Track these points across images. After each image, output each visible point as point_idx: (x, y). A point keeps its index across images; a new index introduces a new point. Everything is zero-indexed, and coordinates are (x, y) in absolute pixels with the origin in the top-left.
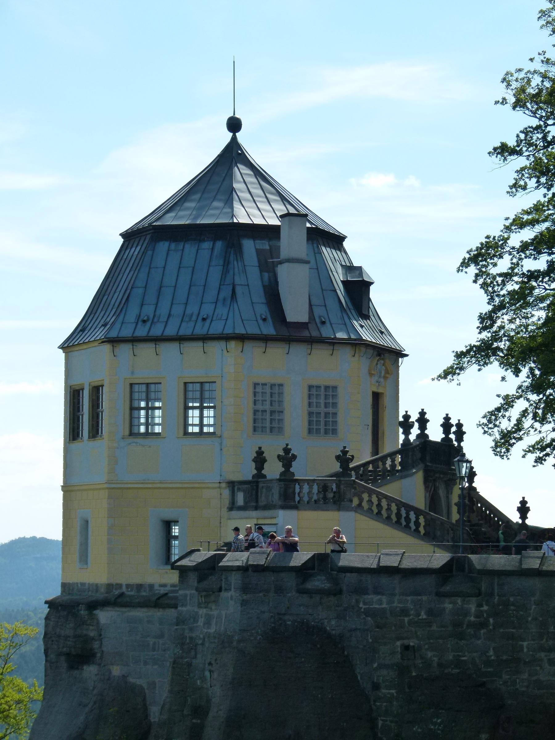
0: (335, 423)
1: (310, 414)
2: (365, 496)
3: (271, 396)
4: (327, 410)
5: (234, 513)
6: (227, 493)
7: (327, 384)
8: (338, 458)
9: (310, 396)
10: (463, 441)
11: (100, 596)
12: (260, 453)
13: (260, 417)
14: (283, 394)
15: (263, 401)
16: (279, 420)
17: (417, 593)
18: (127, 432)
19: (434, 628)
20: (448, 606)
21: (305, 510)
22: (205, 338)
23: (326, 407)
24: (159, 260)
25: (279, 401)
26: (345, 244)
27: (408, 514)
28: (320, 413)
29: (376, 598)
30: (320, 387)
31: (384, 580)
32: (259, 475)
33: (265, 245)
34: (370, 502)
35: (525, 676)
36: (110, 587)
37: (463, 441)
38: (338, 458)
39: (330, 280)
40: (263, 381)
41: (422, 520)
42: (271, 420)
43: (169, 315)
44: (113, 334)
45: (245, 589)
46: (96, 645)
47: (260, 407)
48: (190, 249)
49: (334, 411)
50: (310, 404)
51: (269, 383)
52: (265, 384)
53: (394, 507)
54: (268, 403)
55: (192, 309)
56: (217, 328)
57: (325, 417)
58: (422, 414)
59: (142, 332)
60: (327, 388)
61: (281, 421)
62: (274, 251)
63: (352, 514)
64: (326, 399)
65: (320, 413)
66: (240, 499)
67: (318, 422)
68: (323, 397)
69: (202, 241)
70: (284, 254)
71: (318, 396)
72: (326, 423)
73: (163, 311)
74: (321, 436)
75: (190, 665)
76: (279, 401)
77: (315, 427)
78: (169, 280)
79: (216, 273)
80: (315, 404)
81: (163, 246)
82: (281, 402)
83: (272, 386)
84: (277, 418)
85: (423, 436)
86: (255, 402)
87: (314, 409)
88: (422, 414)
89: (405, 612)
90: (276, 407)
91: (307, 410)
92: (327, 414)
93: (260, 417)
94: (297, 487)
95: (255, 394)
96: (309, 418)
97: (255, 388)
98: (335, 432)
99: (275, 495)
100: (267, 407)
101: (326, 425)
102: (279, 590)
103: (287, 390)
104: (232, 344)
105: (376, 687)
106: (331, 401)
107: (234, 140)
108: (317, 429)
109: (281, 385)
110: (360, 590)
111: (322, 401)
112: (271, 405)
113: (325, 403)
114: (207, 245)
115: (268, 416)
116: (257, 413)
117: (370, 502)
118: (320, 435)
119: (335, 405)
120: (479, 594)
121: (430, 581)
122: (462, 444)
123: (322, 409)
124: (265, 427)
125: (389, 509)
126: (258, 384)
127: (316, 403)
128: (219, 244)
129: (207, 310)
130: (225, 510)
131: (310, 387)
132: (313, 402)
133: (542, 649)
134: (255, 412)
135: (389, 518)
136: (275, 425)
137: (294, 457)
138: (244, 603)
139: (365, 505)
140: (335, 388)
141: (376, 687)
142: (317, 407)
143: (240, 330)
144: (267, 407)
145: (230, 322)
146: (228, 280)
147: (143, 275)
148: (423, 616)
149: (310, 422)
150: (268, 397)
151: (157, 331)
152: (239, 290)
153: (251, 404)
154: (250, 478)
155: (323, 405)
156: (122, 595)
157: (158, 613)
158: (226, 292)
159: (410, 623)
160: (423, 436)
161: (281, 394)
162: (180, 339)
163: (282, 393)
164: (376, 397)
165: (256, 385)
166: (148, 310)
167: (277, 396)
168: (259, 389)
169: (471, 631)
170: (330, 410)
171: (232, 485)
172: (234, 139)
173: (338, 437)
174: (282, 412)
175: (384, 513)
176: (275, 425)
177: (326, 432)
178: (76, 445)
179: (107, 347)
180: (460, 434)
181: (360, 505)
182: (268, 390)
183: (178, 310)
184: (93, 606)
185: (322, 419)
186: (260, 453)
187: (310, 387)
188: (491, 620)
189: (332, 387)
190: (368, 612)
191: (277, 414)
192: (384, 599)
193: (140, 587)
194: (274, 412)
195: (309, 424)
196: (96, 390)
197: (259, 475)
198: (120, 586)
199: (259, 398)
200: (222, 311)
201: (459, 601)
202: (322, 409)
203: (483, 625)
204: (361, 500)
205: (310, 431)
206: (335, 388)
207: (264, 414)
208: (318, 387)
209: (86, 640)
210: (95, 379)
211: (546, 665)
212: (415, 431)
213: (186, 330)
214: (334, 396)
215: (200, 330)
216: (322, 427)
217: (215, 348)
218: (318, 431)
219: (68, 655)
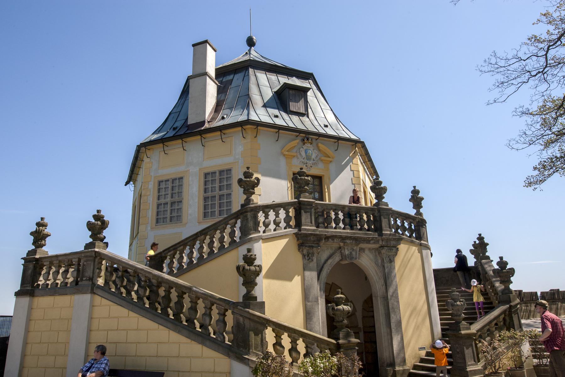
1: (206, 199)
3: (172, 190)
4: (221, 193)
10: (422, 207)
15: (165, 195)
16: (178, 209)
21: (42, 296)
23: (220, 190)
25: (178, 193)
28: (215, 196)
30: (215, 173)
37: (422, 207)
39: (248, 89)
50: (206, 191)
51: (171, 178)
52: (168, 180)
54: (169, 196)
60: (221, 172)
61: (180, 210)
64: (220, 182)
65: (215, 196)
67: (213, 206)
68: (217, 181)
71: (213, 181)
72: (220, 205)
77: (210, 210)
80: (210, 189)
82: (180, 193)
84: (177, 207)
87: (210, 194)
92: (221, 197)
93: (162, 209)
95: (159, 190)
96: (205, 203)
101: (220, 207)
106: (225, 183)
109: (181, 178)
111: (217, 185)
115: (169, 208)
116: (160, 207)
118: (216, 217)
122: (421, 210)
124: (166, 218)
126: (162, 181)
127: (212, 187)
131: (206, 175)
132: (208, 188)
136: (174, 214)
142: (212, 191)
144: (169, 199)
149: (205, 207)
150: (170, 192)
153: (156, 200)
155: (217, 189)
161: (181, 186)
163: (182, 185)
165: (160, 182)
167: (177, 188)
168: (163, 186)
170: (225, 192)
174: (181, 202)
182: (170, 185)
185: (217, 202)
187: (206, 175)
191: (176, 204)
195: (205, 209)
207: (166, 206)
208: (214, 173)
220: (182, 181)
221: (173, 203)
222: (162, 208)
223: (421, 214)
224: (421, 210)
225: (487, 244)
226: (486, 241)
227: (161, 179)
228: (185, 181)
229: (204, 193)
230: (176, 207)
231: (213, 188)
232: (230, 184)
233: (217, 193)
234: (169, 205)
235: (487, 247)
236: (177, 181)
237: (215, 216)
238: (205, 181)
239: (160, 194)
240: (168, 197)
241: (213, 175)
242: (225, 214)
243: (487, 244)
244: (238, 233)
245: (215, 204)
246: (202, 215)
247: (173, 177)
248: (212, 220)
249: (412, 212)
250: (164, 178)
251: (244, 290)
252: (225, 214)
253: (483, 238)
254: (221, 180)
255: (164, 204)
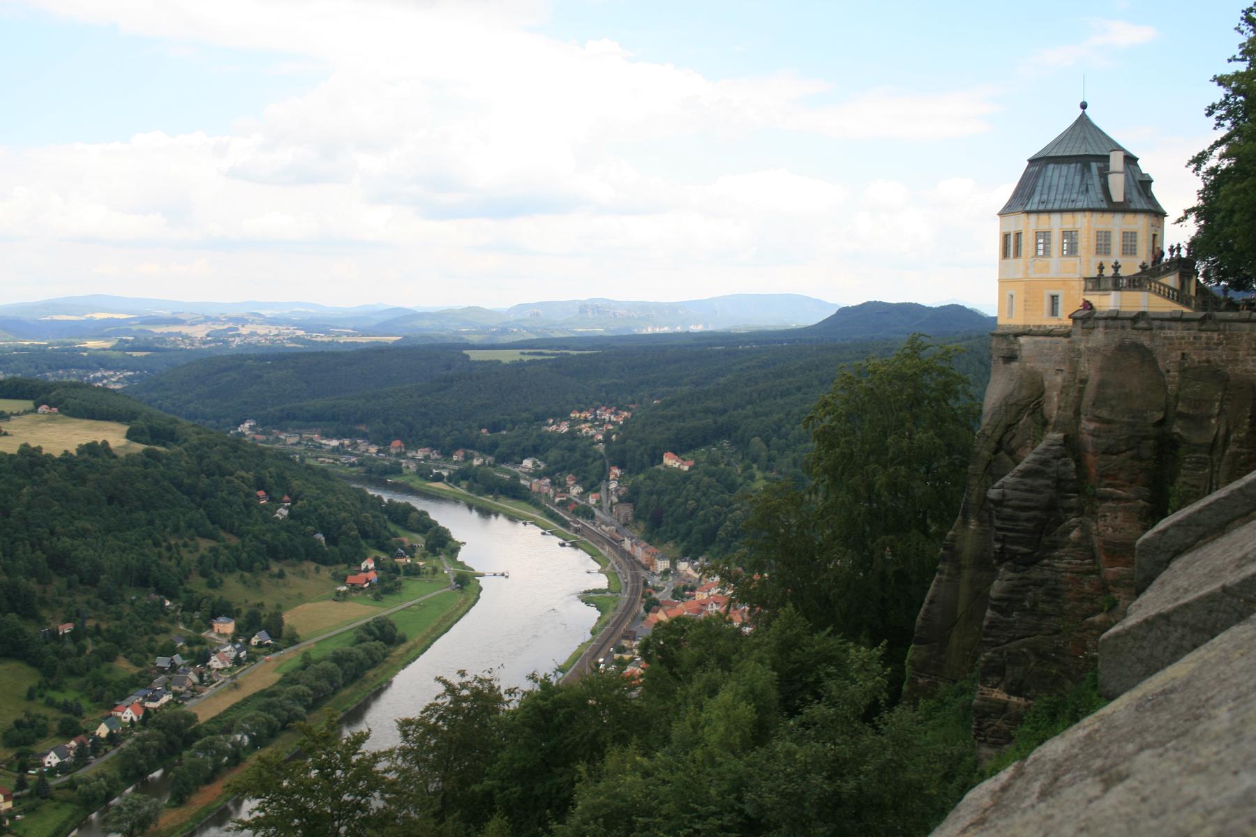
0: (1135, 249)
1: (1124, 245)
2: (1153, 284)
5: (1087, 292)
6: (1083, 283)
8: (1140, 266)
11: (1020, 330)
12: (1101, 264)
17: (1189, 329)
18: (1034, 254)
19: (1197, 345)
20: (1204, 335)
22: (1074, 211)
24: (1049, 173)
26: (1138, 162)
29: (1169, 331)
31: (1173, 324)
32: (1101, 275)
33: (1101, 165)
34: (1155, 287)
35: (1240, 367)
36: (1025, 326)
38: (1140, 266)
41: (1175, 294)
43: (1055, 200)
44: (1028, 208)
45: (1106, 327)
46: (1018, 353)
48: (1064, 168)
50: (1123, 241)
53: (1167, 290)
55: (1066, 196)
56: (1079, 205)
58: (1179, 245)
59: (1042, 207)
60: (1132, 233)
62: (1107, 168)
63: (1146, 293)
66: (1090, 286)
69: (1071, 163)
70: (1112, 169)
71: (1127, 237)
73: (1052, 197)
75: (1078, 361)
78: (1055, 182)
79: (1078, 179)
81: (1051, 166)
82: (1109, 240)
83: (1106, 232)
85: (1179, 255)
88: (1179, 245)
89: (1183, 338)
92: (1131, 245)
94: (1121, 281)
98: (1135, 254)
99: (1110, 283)
102: (1123, 327)
103: (1112, 235)
104: (1087, 214)
105: (1168, 371)
107: (1084, 112)
110: (1162, 328)
111: (1129, 239)
114: (1073, 165)
115: (1103, 247)
117: (1155, 287)
119: (1135, 241)
120: (1218, 330)
121: (1195, 324)
123: (1129, 243)
125: (1164, 291)
128: (1079, 165)
129: (1074, 196)
130: (1082, 292)
131: (1124, 233)
133: (1248, 355)
134: (1097, 245)
135: (1164, 295)
137: (1120, 266)
138: (1106, 333)
139: (1153, 288)
140: (1135, 233)
141: (1168, 371)
143: (1091, 206)
144: (1103, 242)
145: (1086, 202)
146: (1085, 182)
147: (1041, 181)
148: (1191, 340)
149: (1123, 249)
151: (1049, 207)
152: (1090, 187)
154: (1095, 276)
156: (1031, 330)
157: (1049, 339)
158: (1083, 188)
159: (1185, 343)
160: (1179, 255)
162: (1061, 211)
164: (1154, 236)
165: (1098, 232)
166: (1045, 197)
168: (1099, 234)
169: (1215, 347)
170: (1133, 243)
171: (1086, 279)
172: (1084, 112)
175: (1162, 292)
177: (1131, 254)
178: (1006, 261)
179: (1024, 216)
181: (1150, 289)
183: (1059, 197)
184: (1017, 335)
186: (1101, 264)
187: (1124, 233)
188: (1225, 342)
190: (1165, 338)
192: (1173, 332)
193: (1039, 326)
196: (1018, 235)
197: (1101, 275)
198: (1029, 326)
199: (1099, 238)
200: (1081, 197)
201: (1209, 333)
203: (1221, 344)
204: (1151, 286)
206: (1135, 233)
208: (1128, 233)
209: (1014, 351)
210: (1019, 229)
211: (1250, 362)
212: (1175, 253)
213: (1064, 206)
214: (1136, 237)
215: (1071, 206)
216: (1129, 252)
217: (1079, 216)
218: (1127, 254)
219: (1003, 357)
221: (1105, 245)
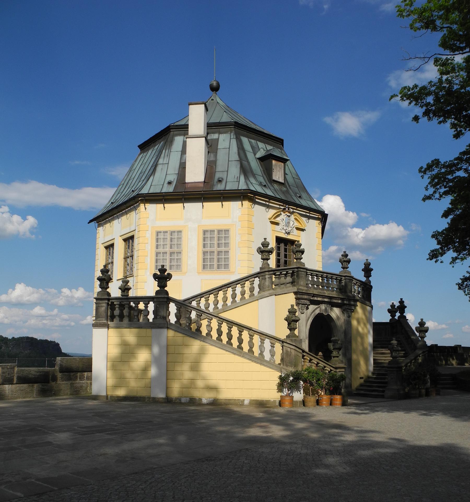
0: (227, 259)
1: (205, 253)
3: (171, 241)
4: (220, 249)
7: (220, 228)
9: (204, 239)
10: (371, 276)
13: (161, 258)
14: (181, 238)
15: (164, 245)
16: (177, 259)
23: (219, 247)
25: (177, 244)
27: (230, 330)
28: (214, 252)
30: (214, 231)
40: (165, 229)
42: (171, 260)
47: (161, 250)
49: (226, 249)
50: (204, 246)
51: (170, 230)
52: (167, 232)
54: (168, 246)
57: (218, 255)
60: (219, 231)
61: (179, 260)
64: (218, 240)
65: (214, 252)
68: (216, 239)
74: (215, 271)
76: (177, 244)
82: (179, 245)
83: (172, 233)
84: (176, 257)
86: (157, 247)
87: (208, 249)
90: (175, 249)
91: (202, 250)
92: (219, 253)
93: (161, 258)
95: (157, 240)
96: (204, 256)
97: (157, 235)
98: (226, 266)
100: (168, 249)
101: (218, 262)
106: (223, 242)
108: (210, 265)
109: (180, 232)
111: (216, 242)
112: (171, 248)
113: (218, 243)
116: (159, 255)
118: (214, 270)
119: (227, 245)
126: (161, 232)
127: (210, 244)
131: (205, 232)
134: (157, 254)
136: (174, 263)
140: (227, 231)
142: (210, 247)
144: (168, 249)
149: (204, 260)
150: (168, 242)
155: (216, 245)
161: (179, 239)
165: (158, 233)
168: (161, 236)
170: (223, 249)
173: (230, 271)
174: (180, 253)
176: (174, 263)
180: (368, 270)
182: (168, 236)
185: (215, 257)
187: (205, 232)
189: (225, 230)
194: (174, 253)
199: (161, 243)
202: (215, 249)
205: (204, 267)
206: (227, 231)
207: (165, 255)
216: (215, 263)
218: (211, 266)
220: (181, 235)
222: (161, 257)
223: (370, 282)
224: (370, 278)
225: (406, 307)
226: (405, 304)
227: (159, 230)
228: (184, 235)
229: (203, 247)
230: (175, 257)
231: (212, 245)
232: (228, 243)
233: (215, 249)
234: (168, 255)
235: (405, 309)
236: (176, 234)
237: (214, 269)
238: (204, 237)
239: (159, 243)
240: (167, 248)
241: (212, 232)
242: (223, 268)
243: (406, 307)
244: (257, 290)
245: (214, 258)
246: (201, 267)
247: (173, 229)
248: (211, 272)
249: (364, 279)
250: (162, 229)
251: (288, 332)
252: (223, 268)
253: (404, 302)
254: (219, 239)
255: (163, 253)
